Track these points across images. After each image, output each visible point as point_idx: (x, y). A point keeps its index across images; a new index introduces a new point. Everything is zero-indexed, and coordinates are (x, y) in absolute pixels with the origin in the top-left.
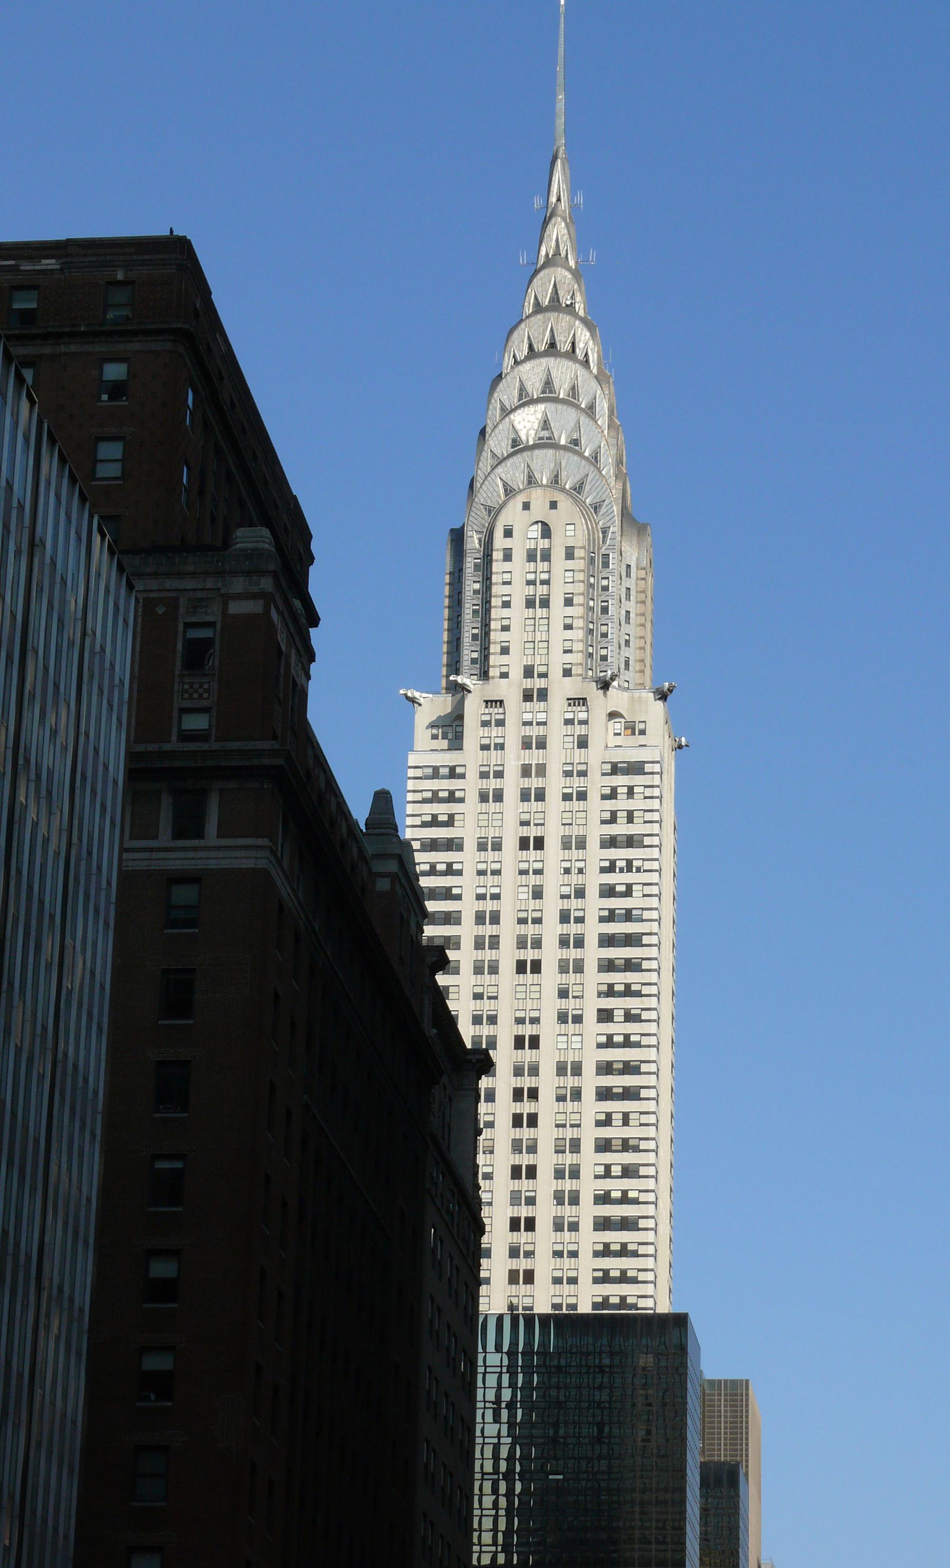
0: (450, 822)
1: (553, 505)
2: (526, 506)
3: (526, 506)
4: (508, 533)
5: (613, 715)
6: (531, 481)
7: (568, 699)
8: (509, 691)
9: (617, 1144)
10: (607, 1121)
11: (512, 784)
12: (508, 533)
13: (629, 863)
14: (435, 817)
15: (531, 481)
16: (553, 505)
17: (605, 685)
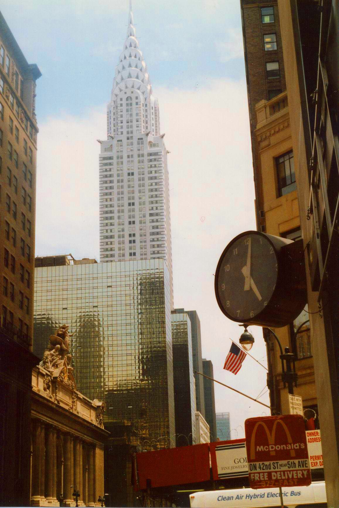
0: (110, 170)
1: (132, 92)
2: (125, 93)
3: (125, 93)
4: (121, 100)
5: (150, 142)
6: (127, 87)
7: (139, 139)
8: (124, 137)
9: (156, 246)
10: (152, 185)
11: (125, 159)
12: (121, 100)
13: (155, 165)
14: (106, 169)
15: (127, 87)
16: (132, 92)
17: (147, 135)
